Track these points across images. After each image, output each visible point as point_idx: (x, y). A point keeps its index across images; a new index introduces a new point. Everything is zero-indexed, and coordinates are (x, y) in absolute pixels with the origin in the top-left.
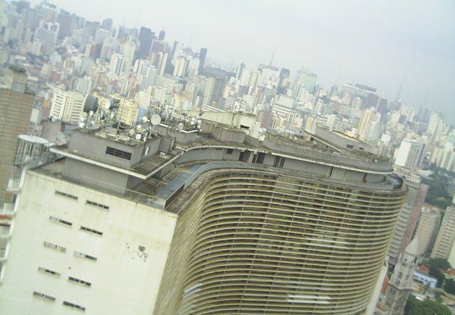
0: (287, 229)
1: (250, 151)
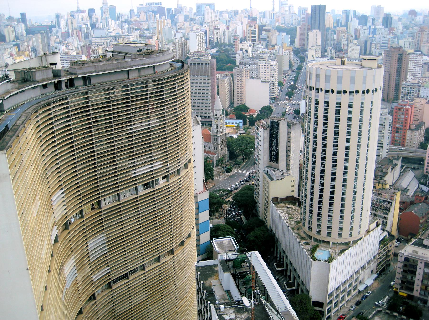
0: (112, 126)
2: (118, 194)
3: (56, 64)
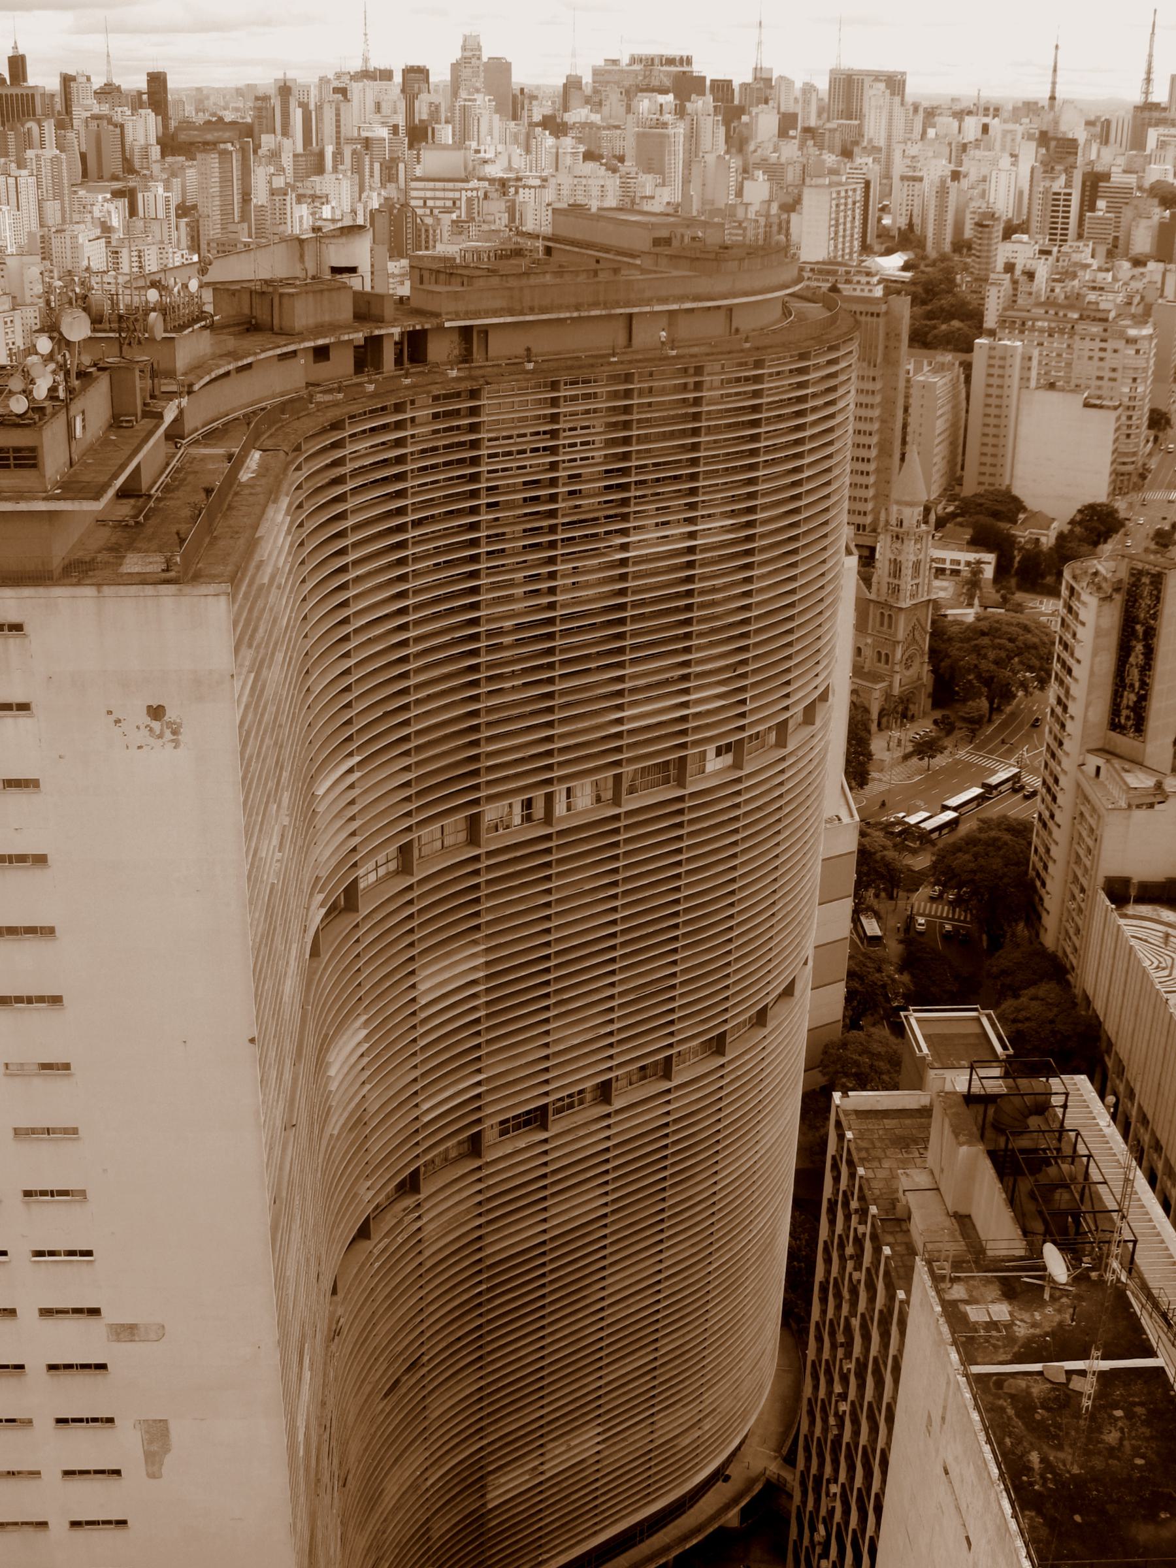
1: (380, 337)
2: (549, 798)
3: (353, 270)
